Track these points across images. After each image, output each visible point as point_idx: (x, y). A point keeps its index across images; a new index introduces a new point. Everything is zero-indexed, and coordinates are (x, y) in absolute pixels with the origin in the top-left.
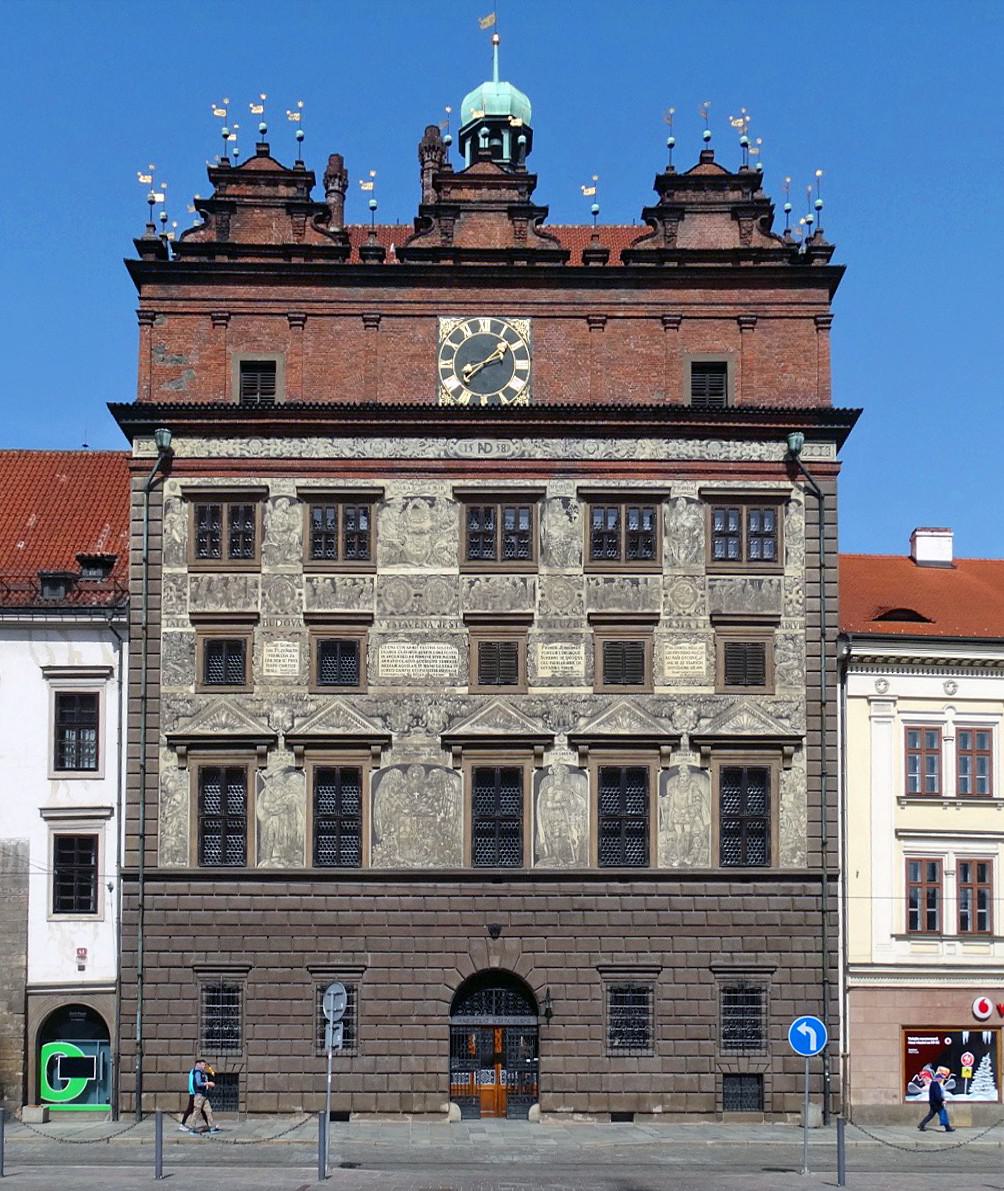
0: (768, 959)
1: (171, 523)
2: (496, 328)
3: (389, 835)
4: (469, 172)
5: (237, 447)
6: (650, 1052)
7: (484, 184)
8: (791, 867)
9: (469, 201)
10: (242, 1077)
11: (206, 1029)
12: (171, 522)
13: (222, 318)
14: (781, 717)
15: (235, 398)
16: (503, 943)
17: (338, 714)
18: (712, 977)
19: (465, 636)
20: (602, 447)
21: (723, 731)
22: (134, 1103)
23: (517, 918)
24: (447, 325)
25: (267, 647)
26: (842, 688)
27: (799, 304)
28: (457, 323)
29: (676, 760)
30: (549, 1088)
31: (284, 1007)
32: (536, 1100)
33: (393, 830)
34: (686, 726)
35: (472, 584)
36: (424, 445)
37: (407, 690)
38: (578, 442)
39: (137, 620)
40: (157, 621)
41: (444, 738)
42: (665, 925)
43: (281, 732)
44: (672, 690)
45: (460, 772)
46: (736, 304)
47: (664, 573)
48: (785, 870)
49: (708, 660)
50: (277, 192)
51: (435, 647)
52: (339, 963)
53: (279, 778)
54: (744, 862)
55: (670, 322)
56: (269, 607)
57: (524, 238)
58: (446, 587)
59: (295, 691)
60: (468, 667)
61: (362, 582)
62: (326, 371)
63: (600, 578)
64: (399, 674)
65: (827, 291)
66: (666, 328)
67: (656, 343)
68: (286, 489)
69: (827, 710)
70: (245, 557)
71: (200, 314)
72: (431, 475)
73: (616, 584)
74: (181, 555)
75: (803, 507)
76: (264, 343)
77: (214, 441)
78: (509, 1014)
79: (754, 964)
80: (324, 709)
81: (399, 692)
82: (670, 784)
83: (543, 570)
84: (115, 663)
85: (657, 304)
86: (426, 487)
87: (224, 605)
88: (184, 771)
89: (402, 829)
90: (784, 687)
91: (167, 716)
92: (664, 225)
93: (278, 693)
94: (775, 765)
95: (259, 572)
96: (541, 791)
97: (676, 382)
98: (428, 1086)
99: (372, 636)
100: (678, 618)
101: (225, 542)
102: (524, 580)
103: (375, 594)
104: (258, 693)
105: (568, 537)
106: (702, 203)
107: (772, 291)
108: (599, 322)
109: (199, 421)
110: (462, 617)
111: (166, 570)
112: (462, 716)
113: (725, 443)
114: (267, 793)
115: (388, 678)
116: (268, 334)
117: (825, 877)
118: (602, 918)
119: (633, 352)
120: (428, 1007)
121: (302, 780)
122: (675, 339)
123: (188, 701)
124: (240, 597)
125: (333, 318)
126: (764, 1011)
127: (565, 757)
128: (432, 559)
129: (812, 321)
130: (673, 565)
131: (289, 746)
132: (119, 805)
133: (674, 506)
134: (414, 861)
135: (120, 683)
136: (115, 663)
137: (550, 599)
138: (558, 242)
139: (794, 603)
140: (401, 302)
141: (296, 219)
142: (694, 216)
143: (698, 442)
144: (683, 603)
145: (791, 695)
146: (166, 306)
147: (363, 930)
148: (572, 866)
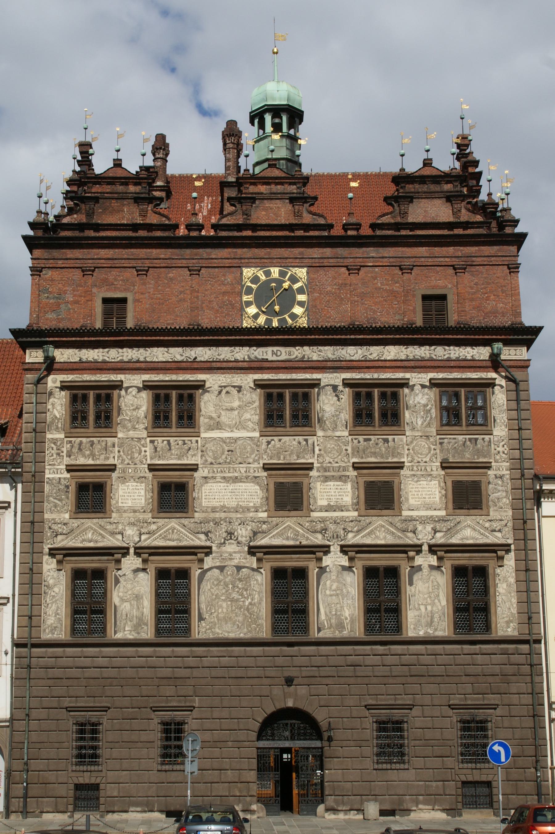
0: (493, 699)
1: (53, 405)
2: (283, 274)
3: (211, 614)
4: (260, 175)
5: (100, 354)
6: (406, 766)
7: (272, 183)
8: (506, 634)
9: (262, 193)
10: (102, 786)
11: (75, 752)
12: (53, 405)
13: (90, 270)
14: (495, 531)
15: (99, 325)
16: (296, 690)
17: (173, 532)
18: (450, 712)
19: (264, 478)
20: (360, 352)
22: (21, 804)
23: (306, 672)
24: (248, 272)
25: (121, 487)
26: (538, 509)
27: (496, 256)
28: (255, 271)
29: (419, 560)
30: (331, 793)
31: (134, 736)
32: (323, 802)
33: (213, 611)
34: (426, 537)
35: (269, 443)
36: (233, 351)
37: (223, 515)
38: (342, 349)
39: (28, 470)
40: (43, 470)
41: (250, 547)
43: (132, 544)
44: (414, 514)
45: (262, 570)
46: (452, 257)
47: (407, 435)
48: (501, 637)
49: (440, 492)
50: (128, 189)
51: (242, 486)
52: (175, 704)
53: (130, 575)
54: (470, 629)
55: (405, 269)
56: (123, 460)
57: (301, 216)
58: (251, 445)
59: (142, 516)
60: (267, 499)
61: (189, 442)
62: (163, 304)
63: (361, 438)
64: (217, 504)
65: (516, 247)
66: (402, 273)
67: (396, 283)
68: (135, 382)
69: (529, 525)
70: (106, 427)
71: (73, 268)
74: (60, 426)
75: (504, 389)
76: (119, 286)
77: (84, 351)
78: (301, 740)
79: (481, 702)
80: (162, 529)
81: (217, 516)
82: (415, 578)
83: (320, 433)
84: (12, 500)
85: (396, 257)
86: (235, 379)
87: (90, 459)
88: (61, 572)
89: (220, 610)
91: (49, 534)
92: (399, 206)
93: (129, 518)
94: (492, 564)
95: (116, 437)
96: (322, 583)
97: (411, 308)
98: (240, 791)
100: (418, 464)
101: (91, 418)
102: (306, 440)
103: (199, 450)
104: (115, 518)
105: (337, 411)
106: (425, 193)
107: (477, 248)
108: (355, 269)
109: (74, 339)
110: (262, 465)
111: (49, 436)
112: (263, 532)
113: (447, 348)
114: (122, 586)
115: (209, 507)
116: (121, 280)
118: (368, 671)
119: (380, 288)
120: (242, 735)
121: (147, 577)
122: (410, 280)
123: (65, 524)
124: (102, 454)
125: (167, 269)
126: (490, 736)
127: (339, 560)
128: (240, 427)
129: (506, 267)
130: (413, 429)
131: (138, 554)
132: (14, 595)
133: (412, 390)
134: (229, 632)
136: (11, 499)
137: (325, 452)
138: (325, 218)
139: (501, 454)
140: (216, 259)
141: (141, 207)
142: (420, 200)
143: (428, 347)
144: (421, 455)
145: (501, 516)
146: (51, 263)
147: (192, 682)
148: (346, 634)
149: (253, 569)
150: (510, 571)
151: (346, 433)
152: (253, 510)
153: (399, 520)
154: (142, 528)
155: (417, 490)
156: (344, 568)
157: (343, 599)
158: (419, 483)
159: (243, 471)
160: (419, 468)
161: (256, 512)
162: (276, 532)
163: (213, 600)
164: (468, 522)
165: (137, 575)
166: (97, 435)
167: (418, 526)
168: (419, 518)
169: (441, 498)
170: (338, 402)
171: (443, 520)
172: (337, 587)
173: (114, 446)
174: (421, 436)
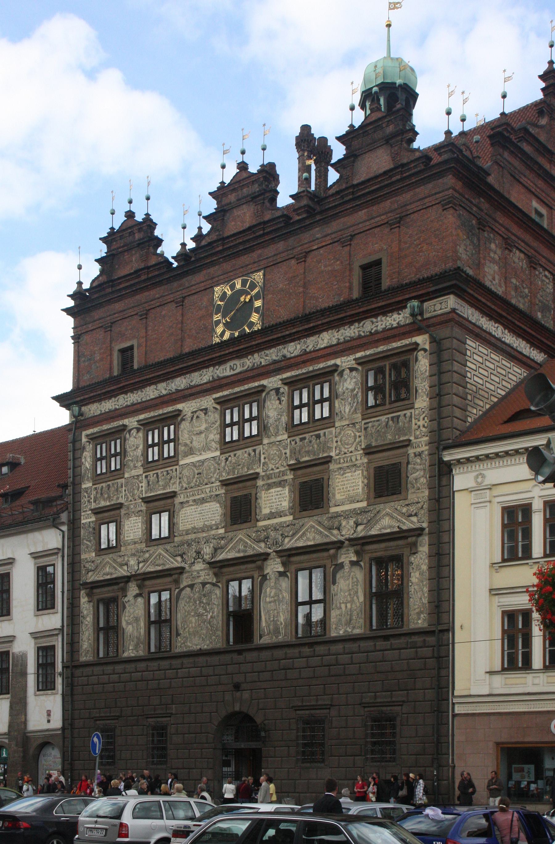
8: (417, 626)
14: (411, 515)
17: (160, 557)
19: (223, 495)
21: (373, 532)
35: (227, 459)
37: (193, 536)
42: (335, 676)
45: (219, 584)
47: (336, 426)
48: (412, 629)
49: (363, 482)
56: (128, 498)
63: (297, 439)
64: (189, 527)
72: (205, 394)
73: (307, 440)
81: (190, 538)
82: (338, 576)
83: (266, 441)
86: (203, 402)
90: (414, 492)
94: (406, 552)
96: (263, 591)
99: (176, 505)
102: (254, 451)
112: (222, 548)
114: (127, 611)
117: (437, 631)
123: (93, 562)
127: (276, 566)
134: (196, 645)
135: (63, 557)
137: (269, 460)
144: (347, 445)
145: (418, 498)
149: (214, 585)
150: (423, 557)
151: (286, 436)
152: (214, 527)
153: (327, 518)
154: (140, 557)
155: (342, 483)
156: (281, 574)
157: (279, 605)
158: (344, 476)
159: (208, 491)
160: (346, 460)
161: (217, 529)
162: (231, 545)
163: (186, 616)
164: (387, 510)
165: (136, 601)
166: (111, 478)
167: (342, 521)
168: (344, 513)
169: (363, 488)
170: (280, 406)
171: (364, 512)
172: (275, 594)
173: (122, 487)
174: (348, 425)
